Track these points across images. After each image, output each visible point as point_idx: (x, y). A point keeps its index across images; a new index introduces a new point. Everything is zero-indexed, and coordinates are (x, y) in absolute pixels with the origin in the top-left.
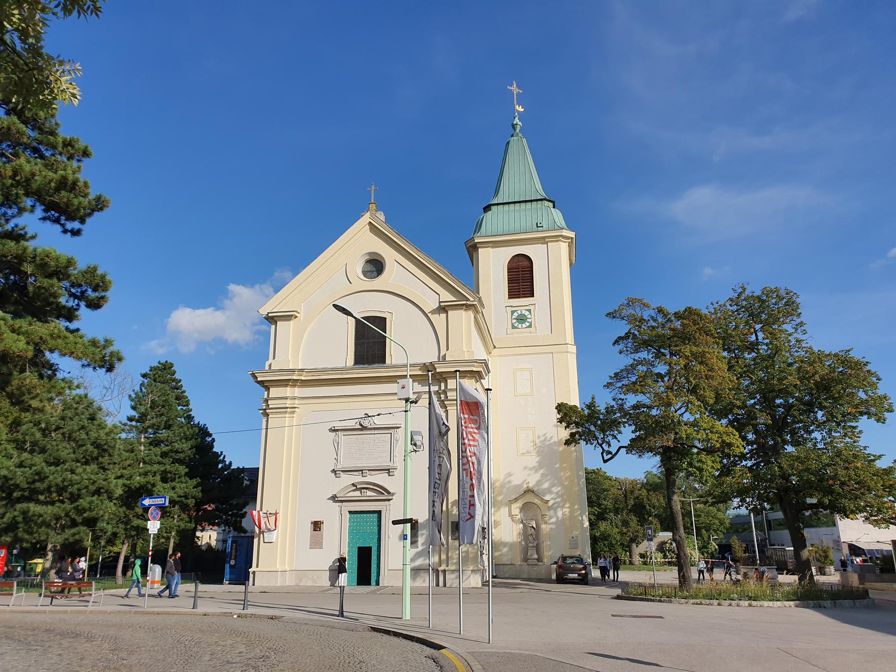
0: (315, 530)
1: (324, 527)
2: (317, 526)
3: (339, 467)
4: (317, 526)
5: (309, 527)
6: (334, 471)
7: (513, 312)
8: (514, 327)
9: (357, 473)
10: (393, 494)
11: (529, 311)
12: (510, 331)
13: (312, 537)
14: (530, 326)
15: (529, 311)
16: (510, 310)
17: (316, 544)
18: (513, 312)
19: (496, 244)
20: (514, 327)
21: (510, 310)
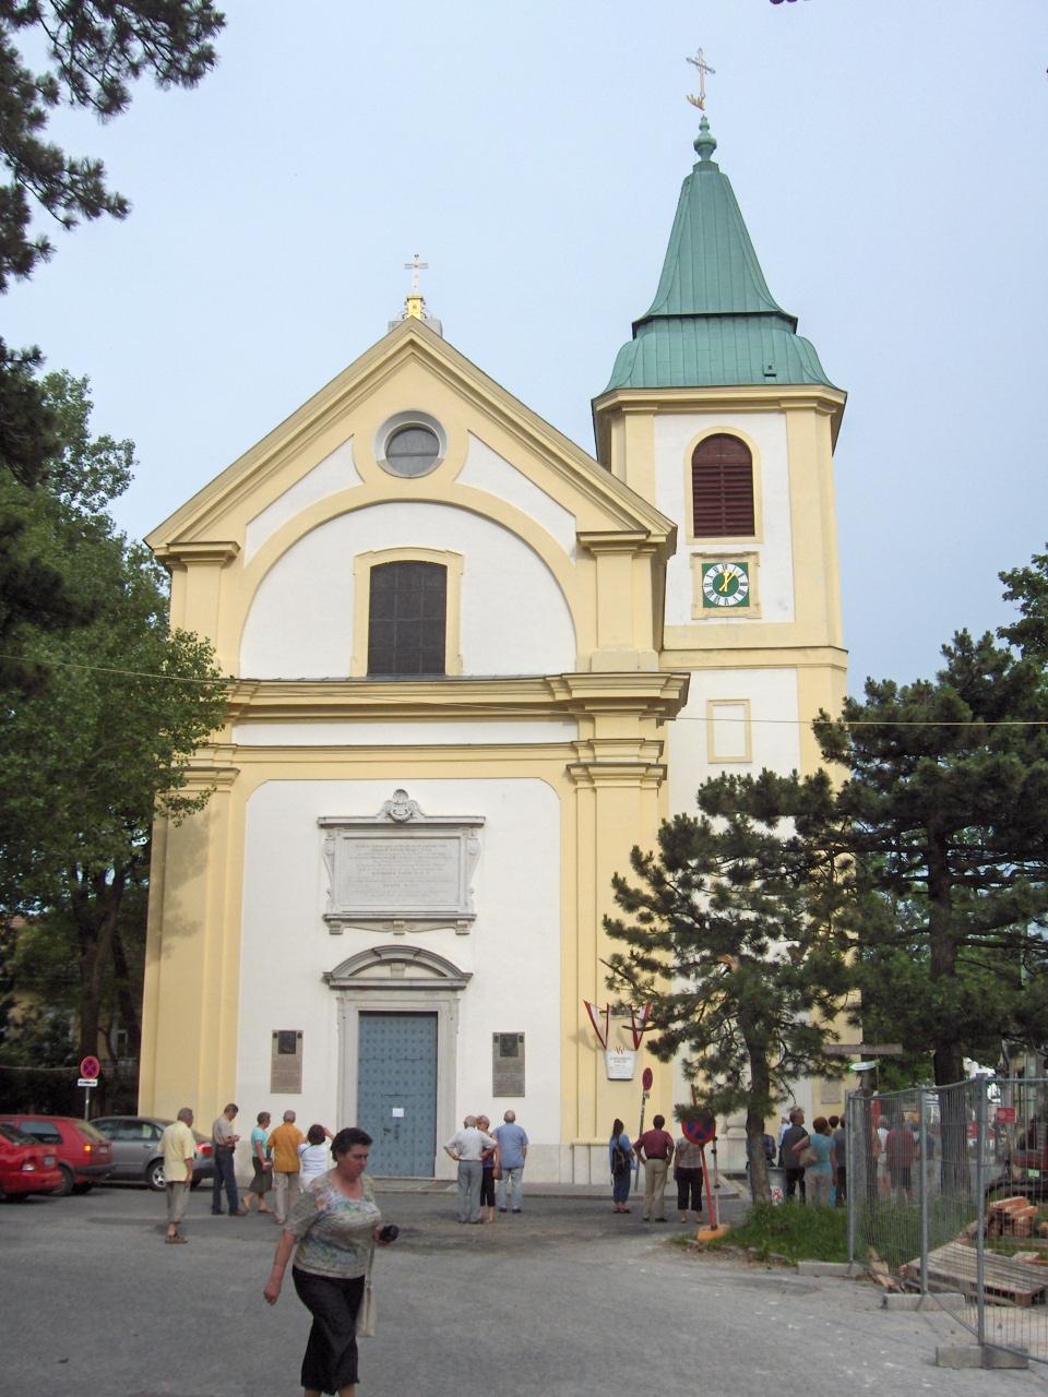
0: (282, 1050)
1: (307, 1046)
2: (287, 1042)
3: (338, 910)
4: (287, 1042)
5: (267, 1046)
6: (327, 920)
7: (706, 568)
8: (708, 604)
9: (379, 926)
10: (467, 977)
11: (744, 567)
12: (702, 611)
13: (276, 1066)
14: (745, 603)
15: (744, 567)
16: (700, 562)
17: (286, 1078)
18: (706, 568)
19: (665, 408)
20: (708, 604)
21: (700, 562)
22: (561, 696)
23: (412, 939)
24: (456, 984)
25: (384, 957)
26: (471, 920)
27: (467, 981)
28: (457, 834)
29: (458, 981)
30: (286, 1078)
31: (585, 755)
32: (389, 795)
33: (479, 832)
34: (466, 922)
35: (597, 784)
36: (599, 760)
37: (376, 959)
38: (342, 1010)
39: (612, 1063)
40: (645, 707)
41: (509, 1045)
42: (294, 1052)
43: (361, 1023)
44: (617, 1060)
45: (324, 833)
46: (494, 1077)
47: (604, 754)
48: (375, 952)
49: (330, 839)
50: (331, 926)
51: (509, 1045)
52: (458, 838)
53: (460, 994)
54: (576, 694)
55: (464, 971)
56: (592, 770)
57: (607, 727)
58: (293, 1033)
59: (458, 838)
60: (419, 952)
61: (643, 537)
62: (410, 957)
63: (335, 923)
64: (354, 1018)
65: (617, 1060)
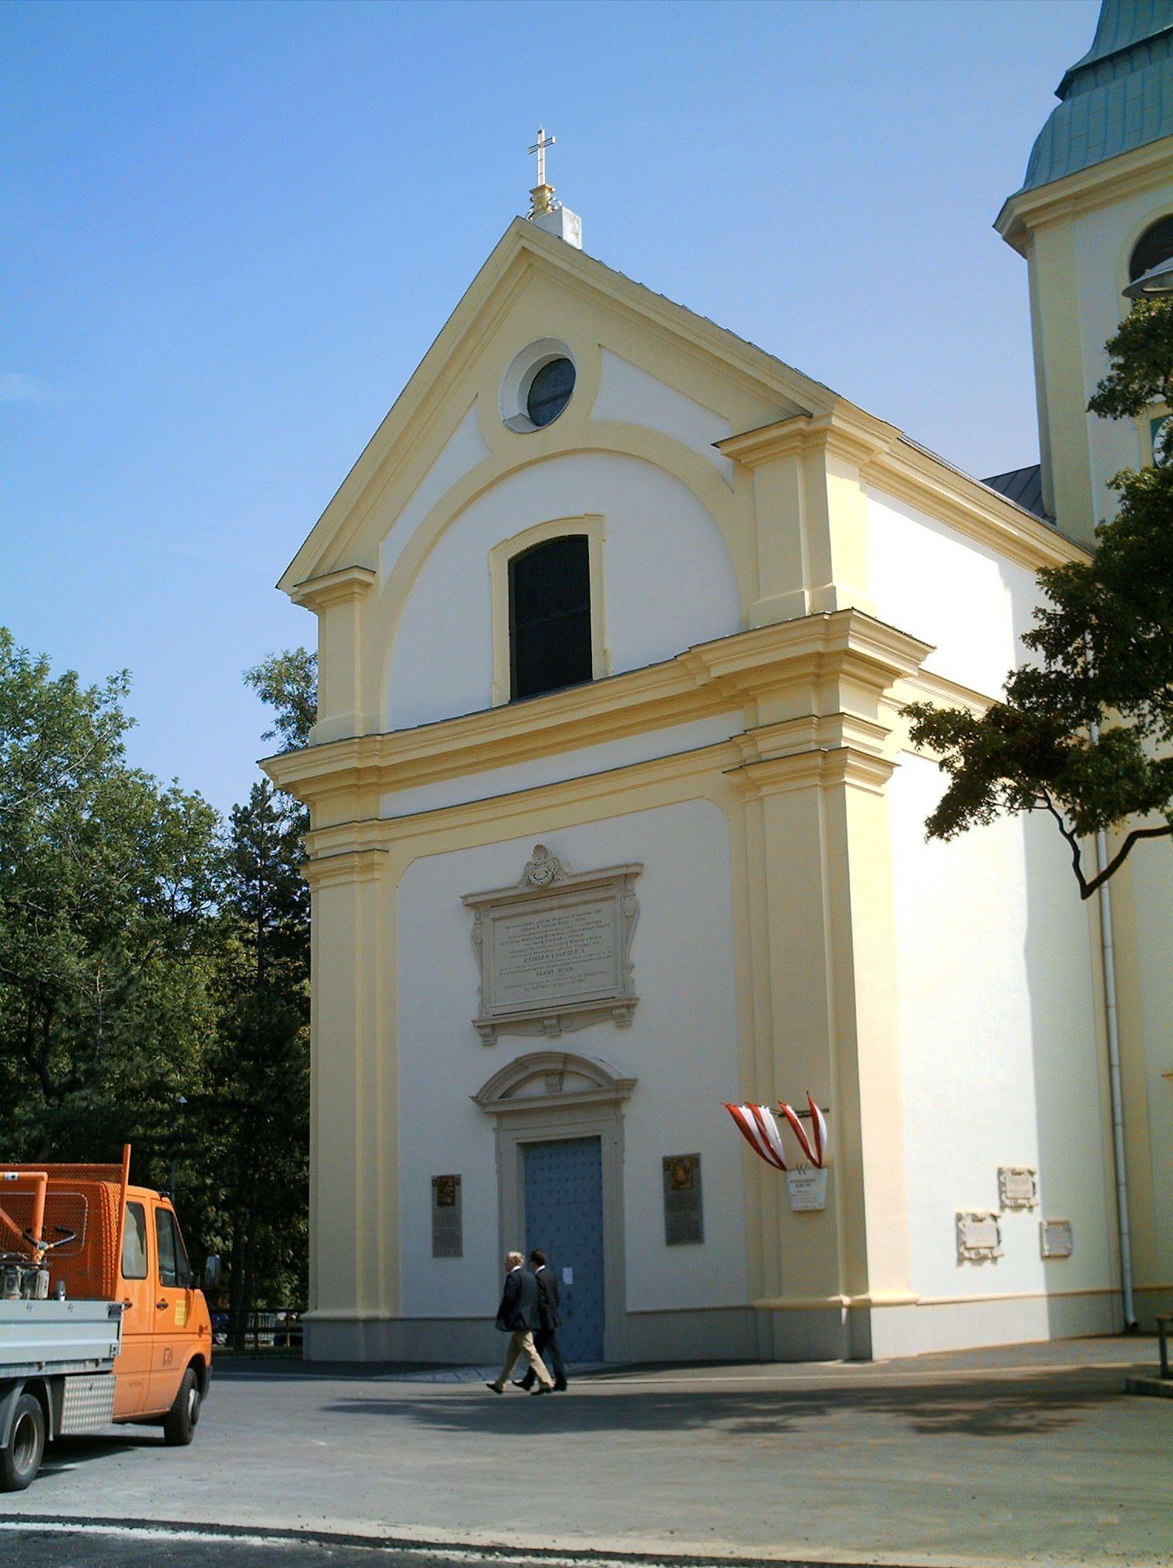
2: (446, 1190)
4: (446, 1190)
10: (629, 1084)
17: (447, 1239)
22: (701, 681)
23: (569, 1043)
24: (611, 1096)
25: (533, 1069)
26: (630, 1006)
27: (629, 1090)
28: (611, 893)
29: (615, 1093)
30: (447, 1239)
31: (748, 753)
32: (528, 856)
33: (640, 887)
34: (624, 1010)
35: (764, 791)
36: (764, 757)
37: (524, 1075)
38: (498, 1145)
39: (793, 1189)
40: (811, 669)
41: (682, 1177)
42: (453, 1203)
43: (526, 1159)
44: (800, 1184)
45: (471, 916)
46: (667, 1219)
47: (767, 745)
48: (520, 1064)
49: (479, 922)
50: (483, 1036)
51: (682, 1177)
52: (613, 898)
53: (625, 1109)
54: (716, 672)
55: (615, 1077)
56: (755, 773)
57: (770, 709)
58: (452, 1177)
59: (613, 898)
60: (567, 1058)
61: (801, 424)
62: (560, 1066)
63: (490, 1030)
64: (513, 1159)
65: (800, 1184)
